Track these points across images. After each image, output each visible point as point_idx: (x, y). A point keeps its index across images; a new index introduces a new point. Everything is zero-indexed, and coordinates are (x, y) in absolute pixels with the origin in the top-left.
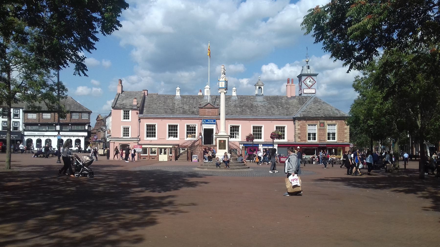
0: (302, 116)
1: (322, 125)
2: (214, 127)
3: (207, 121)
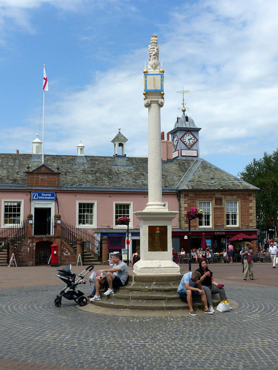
0: (190, 188)
1: (219, 201)
2: (52, 205)
3: (40, 195)
